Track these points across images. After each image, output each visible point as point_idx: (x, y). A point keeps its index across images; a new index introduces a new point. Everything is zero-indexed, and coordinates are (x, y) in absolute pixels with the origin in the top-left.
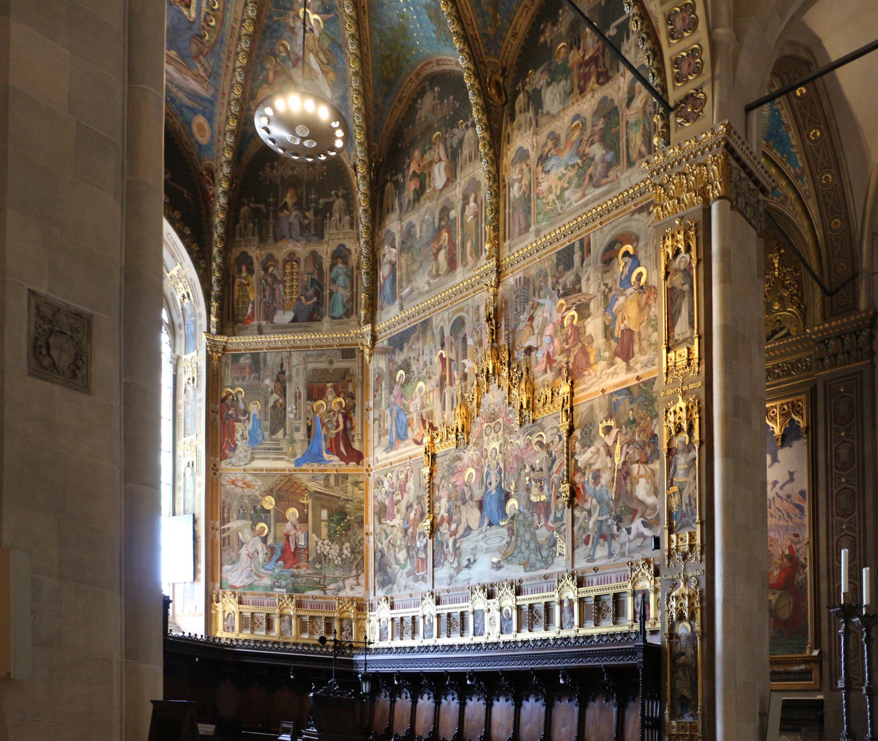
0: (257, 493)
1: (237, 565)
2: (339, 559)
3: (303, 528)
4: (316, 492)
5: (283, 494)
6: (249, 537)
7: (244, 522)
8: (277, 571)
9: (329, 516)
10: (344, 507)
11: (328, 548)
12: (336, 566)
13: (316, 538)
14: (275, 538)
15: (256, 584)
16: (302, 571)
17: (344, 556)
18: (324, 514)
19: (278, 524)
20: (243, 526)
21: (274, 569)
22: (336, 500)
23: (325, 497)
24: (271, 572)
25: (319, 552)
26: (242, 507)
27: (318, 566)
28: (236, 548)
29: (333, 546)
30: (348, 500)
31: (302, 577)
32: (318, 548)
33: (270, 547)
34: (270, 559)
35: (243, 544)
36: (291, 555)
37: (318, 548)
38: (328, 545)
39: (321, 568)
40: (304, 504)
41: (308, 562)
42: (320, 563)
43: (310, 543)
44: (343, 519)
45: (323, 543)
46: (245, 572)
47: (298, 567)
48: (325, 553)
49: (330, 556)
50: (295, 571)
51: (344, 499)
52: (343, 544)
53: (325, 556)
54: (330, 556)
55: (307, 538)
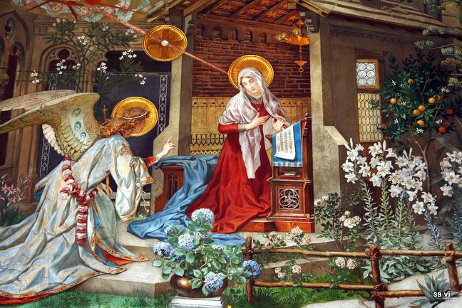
0: (125, 18)
1: (22, 228)
2: (427, 197)
3: (292, 112)
4: (334, 15)
5: (220, 21)
6: (85, 140)
7: (67, 96)
8: (185, 240)
9: (383, 76)
10: (434, 54)
11: (384, 167)
12: (420, 219)
13: (339, 140)
14: (185, 141)
15: (97, 284)
16: (288, 240)
17: (446, 190)
18: (367, 73)
19: (198, 101)
20: (64, 107)
21: (173, 237)
22: (407, 36)
23: (366, 27)
24: (163, 245)
25: (351, 177)
26: (64, 54)
27: (349, 223)
28: (26, 172)
29: (402, 161)
30: (446, 36)
31: (291, 256)
32: (347, 166)
33: (162, 165)
34: (160, 205)
35: (55, 159)
36: (246, 190)
37: (347, 166)
38: (383, 157)
39: (362, 228)
40: (294, 48)
41: (310, 209)
42: (358, 211)
43: (316, 154)
44: (435, 86)
45: (365, 154)
46: (53, 248)
47: (271, 227)
48: (376, 180)
49: (395, 191)
50: (262, 239)
51: (433, 35)
52: (441, 154)
53: (376, 192)
54: (395, 191)
55: (306, 140)
